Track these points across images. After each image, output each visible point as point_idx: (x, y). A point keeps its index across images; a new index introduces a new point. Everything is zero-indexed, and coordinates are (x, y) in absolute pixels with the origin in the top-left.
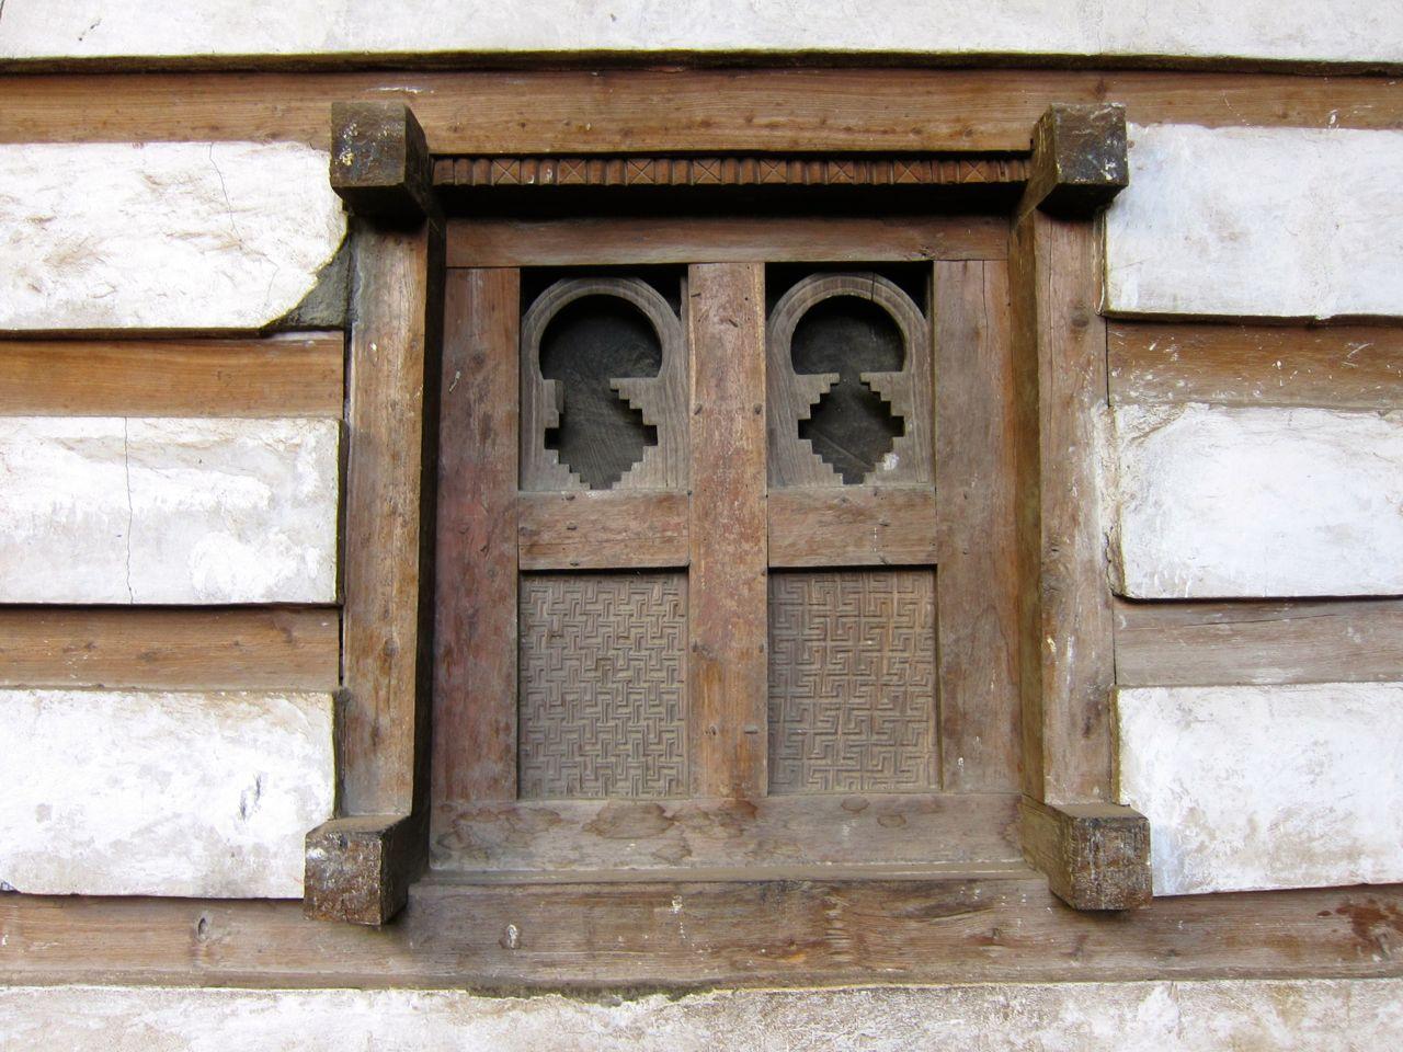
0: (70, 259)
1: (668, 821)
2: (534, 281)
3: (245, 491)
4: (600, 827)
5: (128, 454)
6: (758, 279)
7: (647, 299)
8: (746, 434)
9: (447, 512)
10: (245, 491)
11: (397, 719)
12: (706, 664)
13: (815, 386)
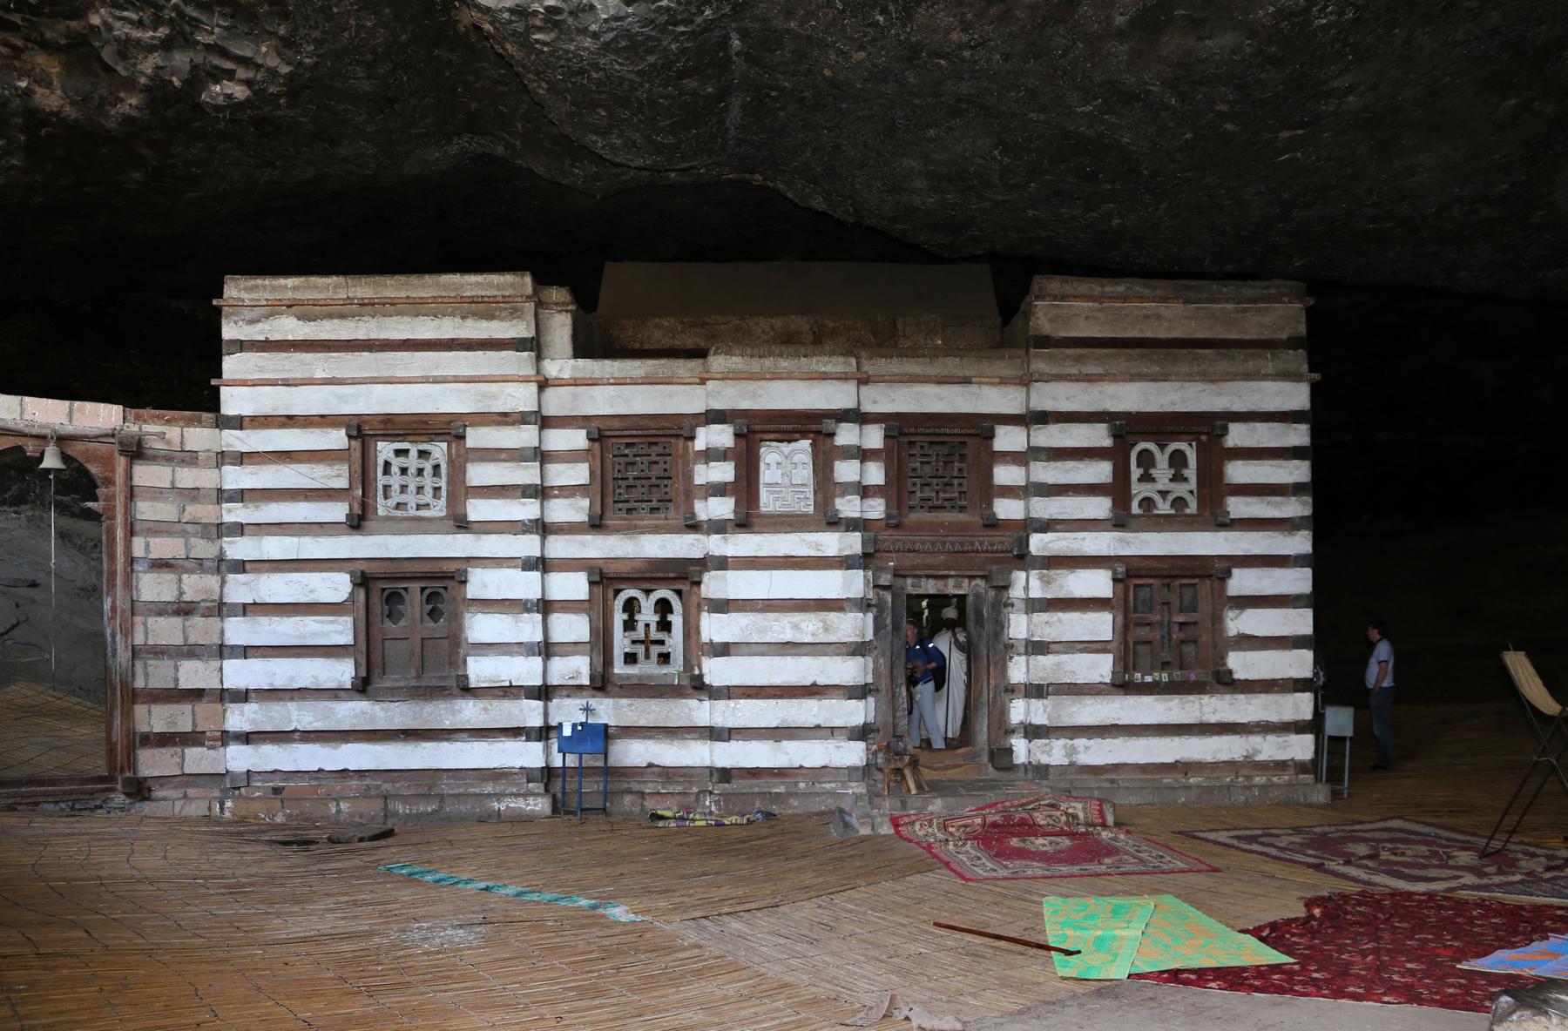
0: (312, 591)
1: (407, 679)
2: (383, 590)
3: (340, 628)
4: (396, 680)
5: (322, 622)
6: (419, 590)
7: (403, 592)
8: (418, 616)
9: (371, 629)
10: (340, 628)
11: (364, 662)
12: (412, 653)
13: (430, 607)
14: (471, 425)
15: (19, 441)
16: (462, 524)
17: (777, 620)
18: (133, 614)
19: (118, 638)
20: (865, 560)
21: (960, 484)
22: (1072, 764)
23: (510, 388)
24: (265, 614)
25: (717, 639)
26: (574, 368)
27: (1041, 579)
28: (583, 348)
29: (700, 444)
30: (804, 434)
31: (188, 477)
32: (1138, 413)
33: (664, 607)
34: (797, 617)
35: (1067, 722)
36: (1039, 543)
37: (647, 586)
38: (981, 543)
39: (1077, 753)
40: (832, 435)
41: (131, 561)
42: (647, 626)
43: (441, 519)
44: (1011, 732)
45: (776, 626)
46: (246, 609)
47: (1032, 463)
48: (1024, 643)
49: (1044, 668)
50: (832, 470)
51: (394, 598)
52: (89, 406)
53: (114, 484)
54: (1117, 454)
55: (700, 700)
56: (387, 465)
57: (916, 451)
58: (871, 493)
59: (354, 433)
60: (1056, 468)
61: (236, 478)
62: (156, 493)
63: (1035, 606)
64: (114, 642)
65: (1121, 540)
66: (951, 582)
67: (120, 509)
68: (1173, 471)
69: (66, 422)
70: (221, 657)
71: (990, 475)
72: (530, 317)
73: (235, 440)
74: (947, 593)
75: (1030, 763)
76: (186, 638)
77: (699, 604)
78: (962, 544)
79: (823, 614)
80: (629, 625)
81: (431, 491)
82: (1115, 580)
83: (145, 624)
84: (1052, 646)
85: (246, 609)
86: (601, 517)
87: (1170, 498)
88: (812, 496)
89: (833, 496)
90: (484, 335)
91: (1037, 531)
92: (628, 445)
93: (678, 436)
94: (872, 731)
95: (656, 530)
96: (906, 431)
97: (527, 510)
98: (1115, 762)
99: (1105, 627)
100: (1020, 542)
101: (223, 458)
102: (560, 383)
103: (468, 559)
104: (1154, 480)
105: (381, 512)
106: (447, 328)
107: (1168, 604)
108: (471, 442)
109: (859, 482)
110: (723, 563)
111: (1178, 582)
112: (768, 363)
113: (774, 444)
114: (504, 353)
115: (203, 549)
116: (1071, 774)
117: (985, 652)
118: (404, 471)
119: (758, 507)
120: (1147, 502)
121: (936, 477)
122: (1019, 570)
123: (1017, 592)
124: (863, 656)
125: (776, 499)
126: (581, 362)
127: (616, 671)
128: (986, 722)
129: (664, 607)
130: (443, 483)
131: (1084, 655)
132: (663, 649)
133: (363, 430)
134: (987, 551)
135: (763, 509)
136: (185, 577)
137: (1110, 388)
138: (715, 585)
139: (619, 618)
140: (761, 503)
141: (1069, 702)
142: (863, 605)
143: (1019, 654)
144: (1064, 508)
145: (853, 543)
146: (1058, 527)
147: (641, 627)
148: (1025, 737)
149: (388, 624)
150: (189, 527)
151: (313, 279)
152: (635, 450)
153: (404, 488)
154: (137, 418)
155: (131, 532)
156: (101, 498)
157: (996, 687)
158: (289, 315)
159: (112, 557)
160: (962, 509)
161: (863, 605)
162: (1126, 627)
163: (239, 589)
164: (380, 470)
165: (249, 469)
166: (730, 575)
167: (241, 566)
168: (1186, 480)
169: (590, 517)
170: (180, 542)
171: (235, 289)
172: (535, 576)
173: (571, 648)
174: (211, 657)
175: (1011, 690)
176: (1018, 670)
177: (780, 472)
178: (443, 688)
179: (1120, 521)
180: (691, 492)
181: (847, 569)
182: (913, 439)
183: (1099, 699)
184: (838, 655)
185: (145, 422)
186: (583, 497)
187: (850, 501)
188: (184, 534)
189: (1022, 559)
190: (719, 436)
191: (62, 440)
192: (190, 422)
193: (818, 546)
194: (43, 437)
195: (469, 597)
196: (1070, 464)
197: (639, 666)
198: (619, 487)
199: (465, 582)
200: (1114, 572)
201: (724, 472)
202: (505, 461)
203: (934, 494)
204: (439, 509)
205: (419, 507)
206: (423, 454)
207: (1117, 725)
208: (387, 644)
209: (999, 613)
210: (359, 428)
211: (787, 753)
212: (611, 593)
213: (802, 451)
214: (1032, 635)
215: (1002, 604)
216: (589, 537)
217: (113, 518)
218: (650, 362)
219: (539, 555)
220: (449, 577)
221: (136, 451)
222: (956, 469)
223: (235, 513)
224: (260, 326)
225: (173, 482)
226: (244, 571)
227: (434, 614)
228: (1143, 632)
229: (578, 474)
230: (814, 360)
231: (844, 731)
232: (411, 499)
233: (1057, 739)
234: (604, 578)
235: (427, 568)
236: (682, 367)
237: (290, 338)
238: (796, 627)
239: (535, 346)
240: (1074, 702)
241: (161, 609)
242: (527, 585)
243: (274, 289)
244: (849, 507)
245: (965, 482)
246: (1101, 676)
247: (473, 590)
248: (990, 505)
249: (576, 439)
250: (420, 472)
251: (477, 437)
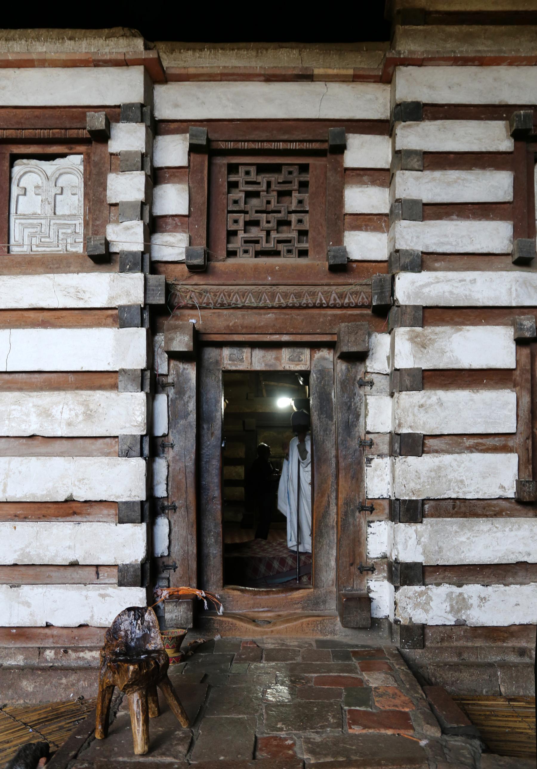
17: (17, 402)
21: (300, 221)
22: (460, 624)
38: (326, 294)
39: (469, 607)
48: (387, 438)
57: (240, 177)
58: (169, 227)
60: (434, 179)
65: (525, 283)
66: (285, 353)
71: (340, 201)
74: (280, 368)
75: (396, 621)
78: (298, 295)
79: (85, 394)
82: (520, 342)
84: (430, 442)
88: (80, 230)
91: (405, 268)
94: (167, 567)
98: (525, 622)
99: (506, 412)
100: (382, 287)
116: (459, 639)
117: (333, 453)
121: (268, 212)
128: (334, 552)
131: (477, 456)
134: (334, 307)
141: (455, 528)
143: (380, 456)
144: (446, 236)
146: (437, 265)
148: (391, 579)
157: (347, 504)
160: (303, 253)
181: (122, 326)
183: (499, 522)
184: (107, 455)
187: (127, 228)
193: (78, 293)
196: (453, 174)
203: (263, 234)
207: (526, 563)
209: (353, 395)
211: (28, 604)
214: (400, 425)
222: (294, 202)
231: (115, 570)
233: (438, 585)
238: (45, 413)
240: (462, 527)
245: (306, 218)
246: (502, 487)
248: (339, 241)
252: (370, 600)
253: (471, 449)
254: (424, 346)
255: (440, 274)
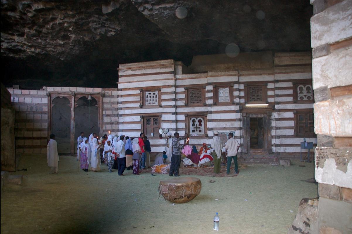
0: (134, 119)
2: (147, 119)
5: (136, 125)
8: (153, 124)
10: (138, 126)
13: (155, 122)
14: (162, 88)
15: (85, 95)
16: (161, 106)
18: (103, 124)
19: (101, 128)
20: (240, 111)
23: (169, 81)
24: (125, 124)
25: (210, 127)
26: (182, 76)
27: (278, 114)
28: (183, 73)
29: (206, 90)
30: (227, 87)
31: (112, 100)
32: (299, 79)
33: (200, 121)
34: (226, 123)
35: (284, 143)
36: (277, 107)
37: (196, 117)
40: (233, 86)
41: (103, 115)
42: (197, 125)
43: (157, 106)
44: (272, 145)
45: (222, 124)
46: (122, 123)
47: (275, 91)
49: (280, 132)
50: (233, 94)
51: (148, 121)
52: (96, 88)
53: (100, 102)
54: (294, 88)
55: (207, 139)
56: (147, 96)
59: (141, 90)
61: (121, 100)
62: (107, 103)
63: (277, 120)
64: (100, 129)
67: (101, 106)
68: (307, 91)
69: (92, 91)
70: (118, 132)
72: (173, 67)
73: (120, 93)
76: (112, 128)
77: (207, 120)
80: (193, 125)
81: (155, 101)
82: (294, 114)
83: (105, 126)
85: (122, 123)
86: (187, 104)
87: (307, 97)
89: (233, 99)
90: (165, 71)
92: (193, 90)
93: (202, 88)
95: (198, 106)
96: (249, 85)
97: (173, 103)
101: (118, 96)
102: (179, 79)
103: (162, 113)
104: (303, 93)
105: (146, 105)
106: (158, 70)
107: (307, 119)
108: (162, 91)
109: (239, 96)
110: (211, 112)
111: (309, 114)
112: (220, 73)
113: (222, 89)
114: (168, 74)
115: (115, 112)
118: (150, 97)
119: (218, 101)
120: (301, 98)
122: (273, 112)
123: (273, 117)
124: (240, 130)
125: (222, 99)
126: (183, 75)
127: (191, 133)
129: (200, 121)
130: (157, 99)
131: (288, 130)
132: (200, 129)
133: (143, 90)
135: (219, 102)
136: (112, 117)
137: (292, 75)
138: (210, 117)
139: (191, 123)
140: (219, 100)
142: (240, 120)
143: (274, 129)
145: (237, 108)
147: (196, 125)
149: (148, 125)
150: (113, 109)
151: (134, 64)
152: (194, 91)
153: (150, 100)
154: (104, 90)
155: (103, 110)
156: (98, 104)
158: (130, 70)
159: (100, 114)
161: (240, 120)
162: (297, 124)
163: (121, 119)
164: (146, 97)
165: (123, 98)
166: (212, 114)
167: (122, 115)
168: (310, 93)
169: (185, 104)
170: (111, 111)
171: (121, 67)
172: (174, 116)
173: (182, 129)
174: (116, 132)
175: (272, 137)
176: (274, 133)
177: (223, 94)
178: (157, 137)
179: (295, 102)
180: (205, 99)
182: (250, 86)
185: (105, 91)
186: (184, 100)
188: (112, 110)
189: (274, 110)
190: (210, 88)
191: (91, 94)
192: (113, 90)
194: (88, 94)
195: (162, 120)
197: (195, 132)
198: (191, 98)
199: (161, 117)
200: (294, 112)
201: (211, 95)
202: (169, 94)
204: (157, 104)
205: (153, 103)
206: (154, 94)
208: (147, 129)
210: (142, 89)
212: (190, 118)
213: (227, 90)
215: (270, 120)
216: (185, 108)
217: (100, 108)
218: (197, 74)
219: (175, 112)
220: (158, 116)
221: (104, 96)
223: (120, 106)
224: (125, 73)
225: (110, 101)
226: (122, 116)
227: (156, 123)
228: (301, 125)
229: (183, 96)
230: (229, 72)
232: (152, 102)
233: (282, 147)
234: (188, 116)
235: (154, 115)
236: (203, 75)
237: (130, 74)
239: (175, 73)
240: (286, 139)
241: (108, 123)
242: (173, 117)
243: (127, 66)
244: (237, 100)
247: (163, 119)
249: (183, 89)
250: (153, 97)
251: (163, 90)
252: (272, 149)
253: (287, 129)
254: (279, 115)
255: (282, 105)
